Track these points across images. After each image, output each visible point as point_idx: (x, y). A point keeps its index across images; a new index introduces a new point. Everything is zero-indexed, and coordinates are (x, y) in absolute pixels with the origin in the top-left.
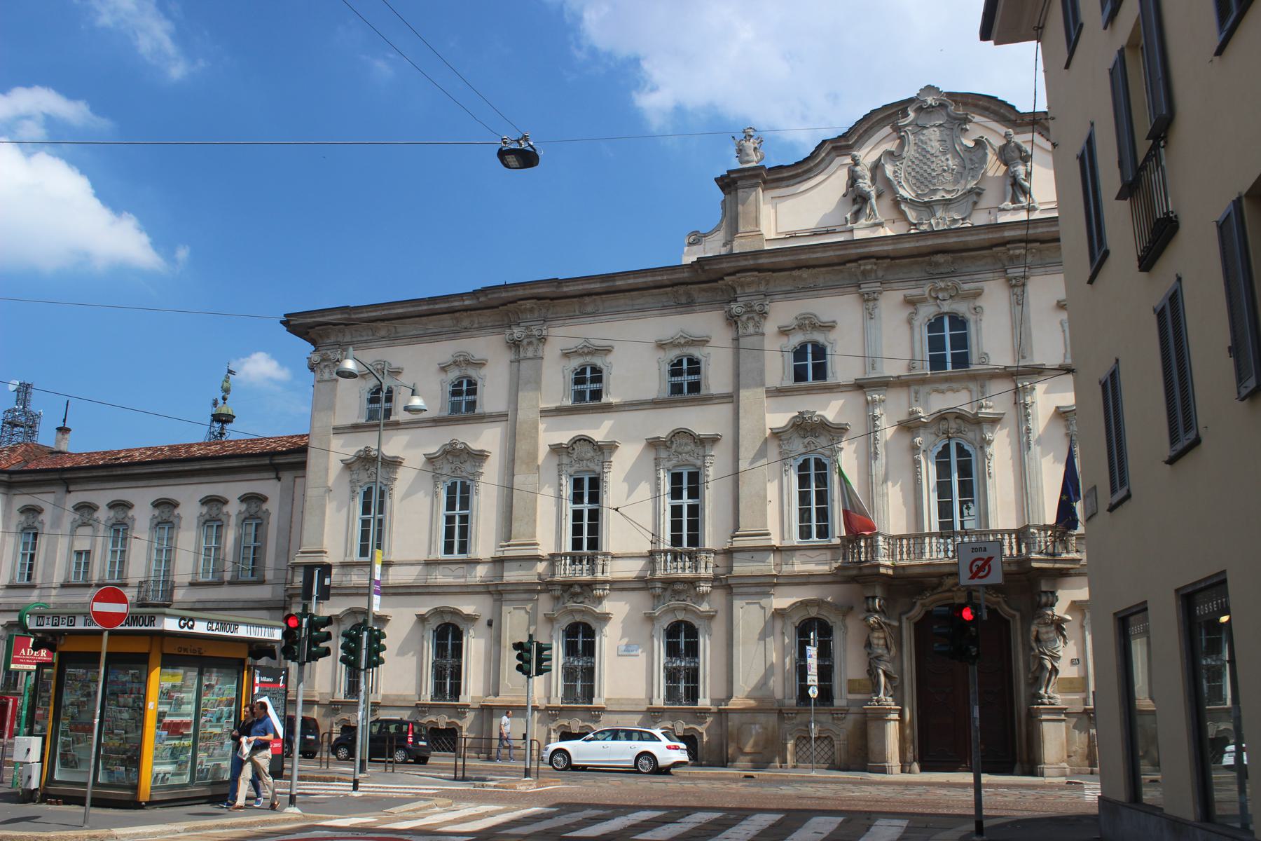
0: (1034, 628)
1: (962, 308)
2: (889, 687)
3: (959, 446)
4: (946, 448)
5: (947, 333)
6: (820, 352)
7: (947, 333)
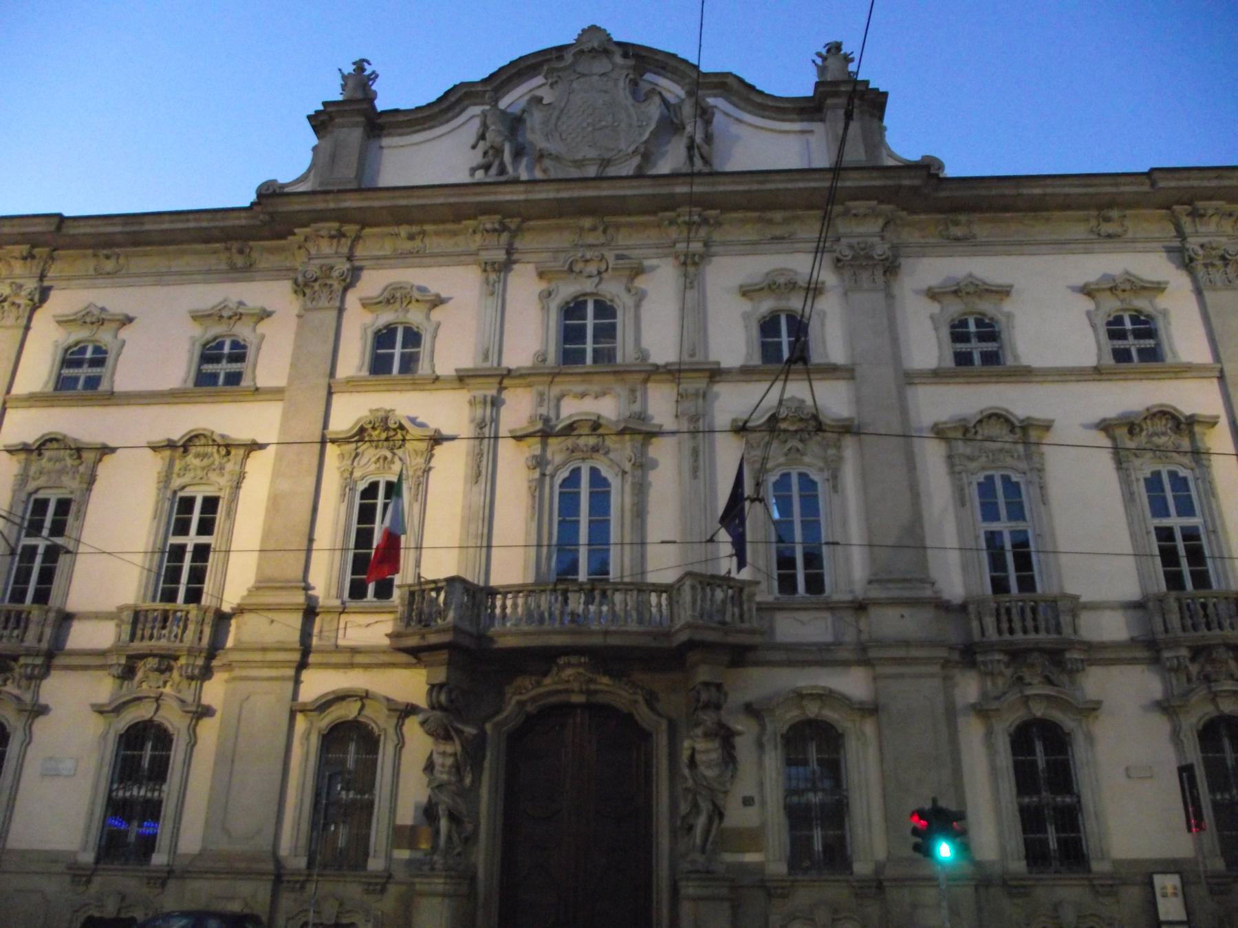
0: (687, 744)
1: (612, 289)
2: (455, 837)
3: (594, 472)
4: (576, 473)
5: (590, 322)
6: (413, 337)
7: (590, 322)
